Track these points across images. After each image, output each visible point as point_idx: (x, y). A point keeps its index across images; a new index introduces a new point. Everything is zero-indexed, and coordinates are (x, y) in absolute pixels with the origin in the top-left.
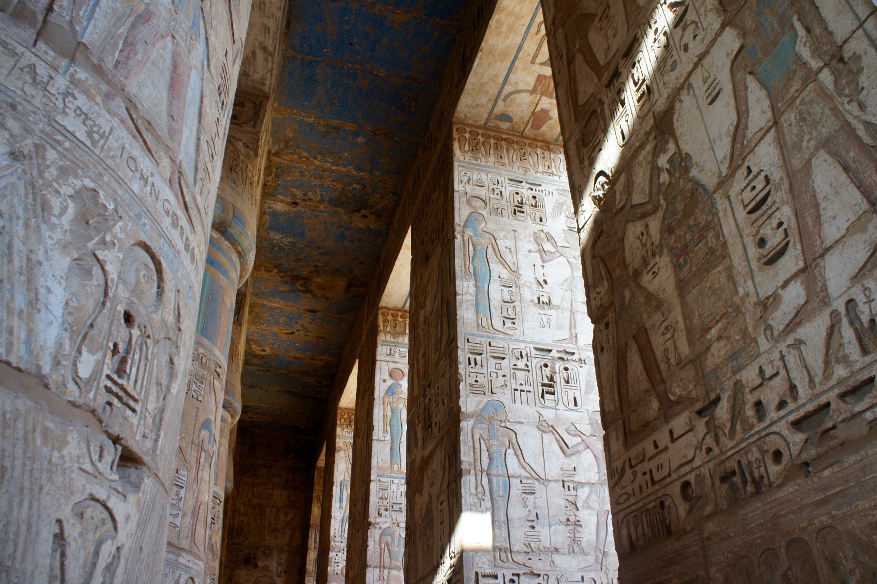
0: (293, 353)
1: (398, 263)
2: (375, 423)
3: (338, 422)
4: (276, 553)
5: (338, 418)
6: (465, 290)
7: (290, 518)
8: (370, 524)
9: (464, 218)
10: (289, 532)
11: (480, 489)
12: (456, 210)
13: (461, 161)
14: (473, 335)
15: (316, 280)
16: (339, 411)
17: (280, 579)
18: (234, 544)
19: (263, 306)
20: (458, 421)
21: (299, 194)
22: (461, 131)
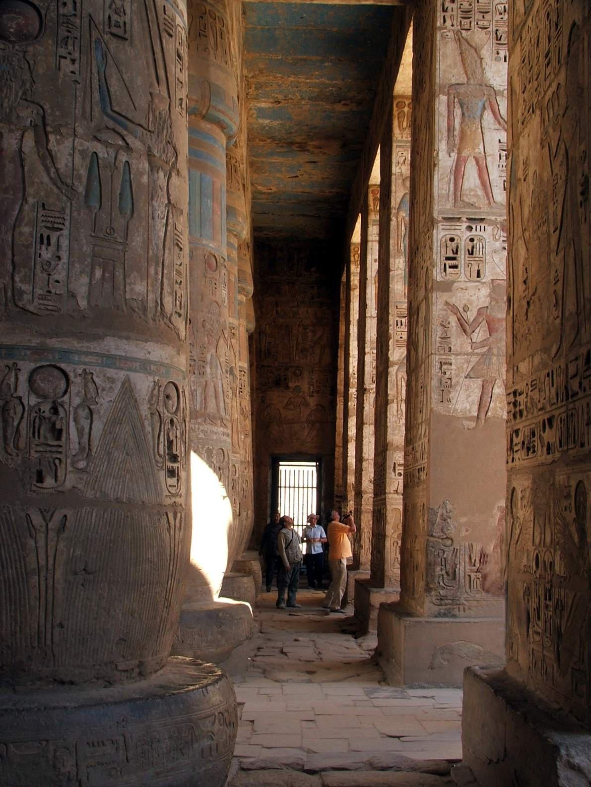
0: (300, 190)
1: (374, 168)
2: (368, 302)
3: (352, 259)
4: (306, 374)
5: (352, 254)
6: (396, 266)
7: (318, 336)
8: (365, 389)
9: (399, 200)
10: (318, 351)
11: (399, 412)
12: (393, 194)
13: (399, 141)
14: (401, 302)
15: (311, 143)
16: (352, 247)
17: (312, 399)
18: (263, 366)
19: (262, 162)
20: (387, 367)
21: (280, 97)
22: (400, 105)
